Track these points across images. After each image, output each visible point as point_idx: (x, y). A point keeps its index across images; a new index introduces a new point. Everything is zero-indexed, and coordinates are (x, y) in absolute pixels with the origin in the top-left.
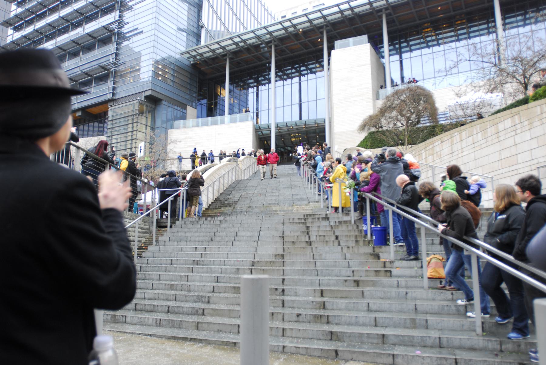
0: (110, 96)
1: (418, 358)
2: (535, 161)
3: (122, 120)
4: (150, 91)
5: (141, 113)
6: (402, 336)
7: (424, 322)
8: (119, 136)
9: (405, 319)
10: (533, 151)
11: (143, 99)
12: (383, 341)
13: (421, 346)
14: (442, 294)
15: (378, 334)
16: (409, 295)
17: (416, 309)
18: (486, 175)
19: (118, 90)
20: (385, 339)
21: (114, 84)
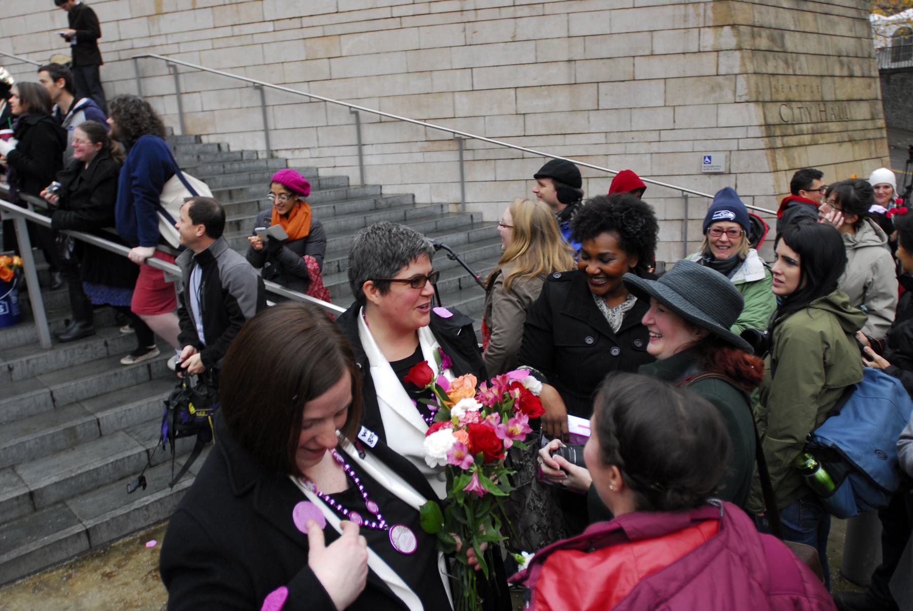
1: (137, 513)
2: (127, 45)
6: (72, 478)
7: (94, 426)
9: (53, 435)
10: (120, 23)
12: (34, 504)
13: (114, 481)
14: (89, 350)
15: (17, 498)
16: (17, 371)
17: (54, 400)
18: (24, 57)
20: (37, 500)
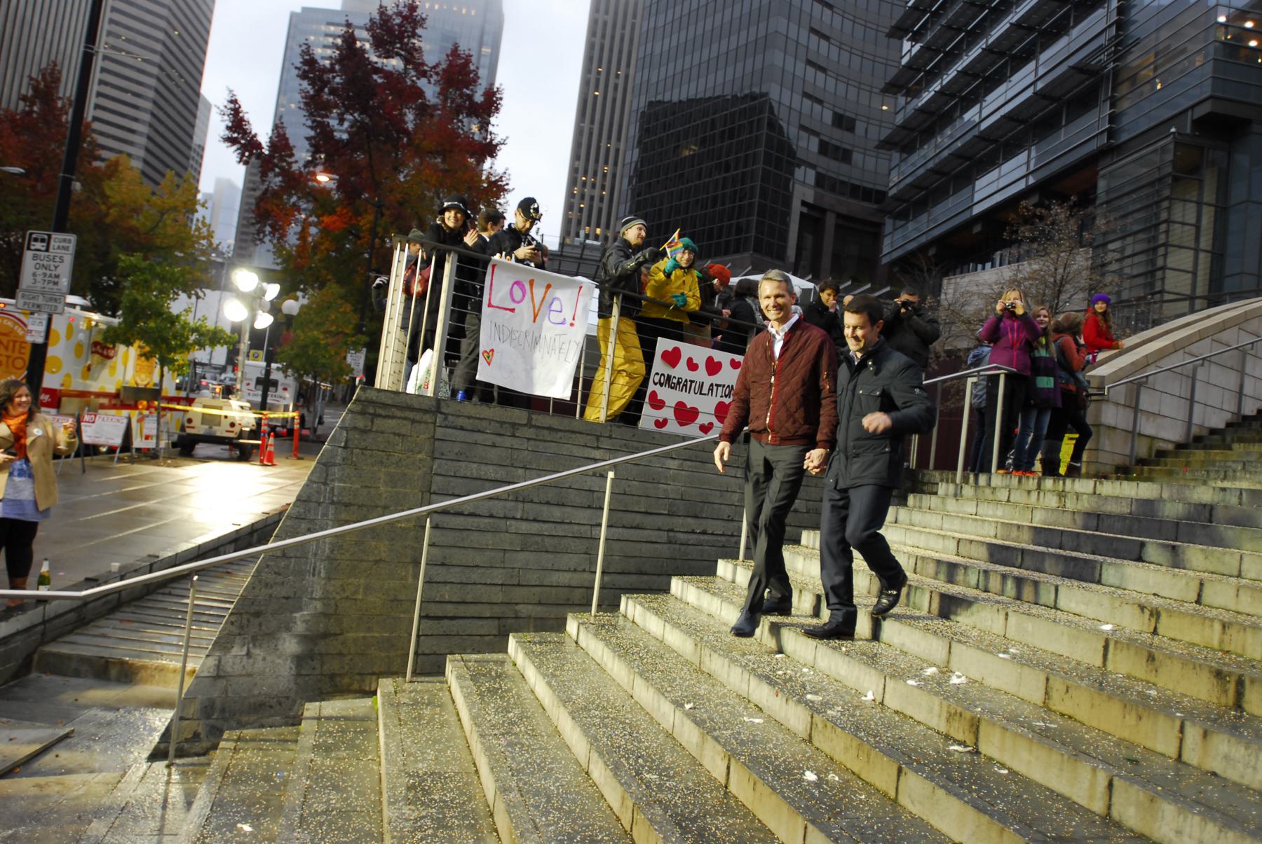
0: (1104, 139)
3: (1126, 200)
4: (1210, 102)
5: (1186, 172)
8: (1129, 240)
11: (1188, 131)
19: (1125, 121)
21: (1112, 106)
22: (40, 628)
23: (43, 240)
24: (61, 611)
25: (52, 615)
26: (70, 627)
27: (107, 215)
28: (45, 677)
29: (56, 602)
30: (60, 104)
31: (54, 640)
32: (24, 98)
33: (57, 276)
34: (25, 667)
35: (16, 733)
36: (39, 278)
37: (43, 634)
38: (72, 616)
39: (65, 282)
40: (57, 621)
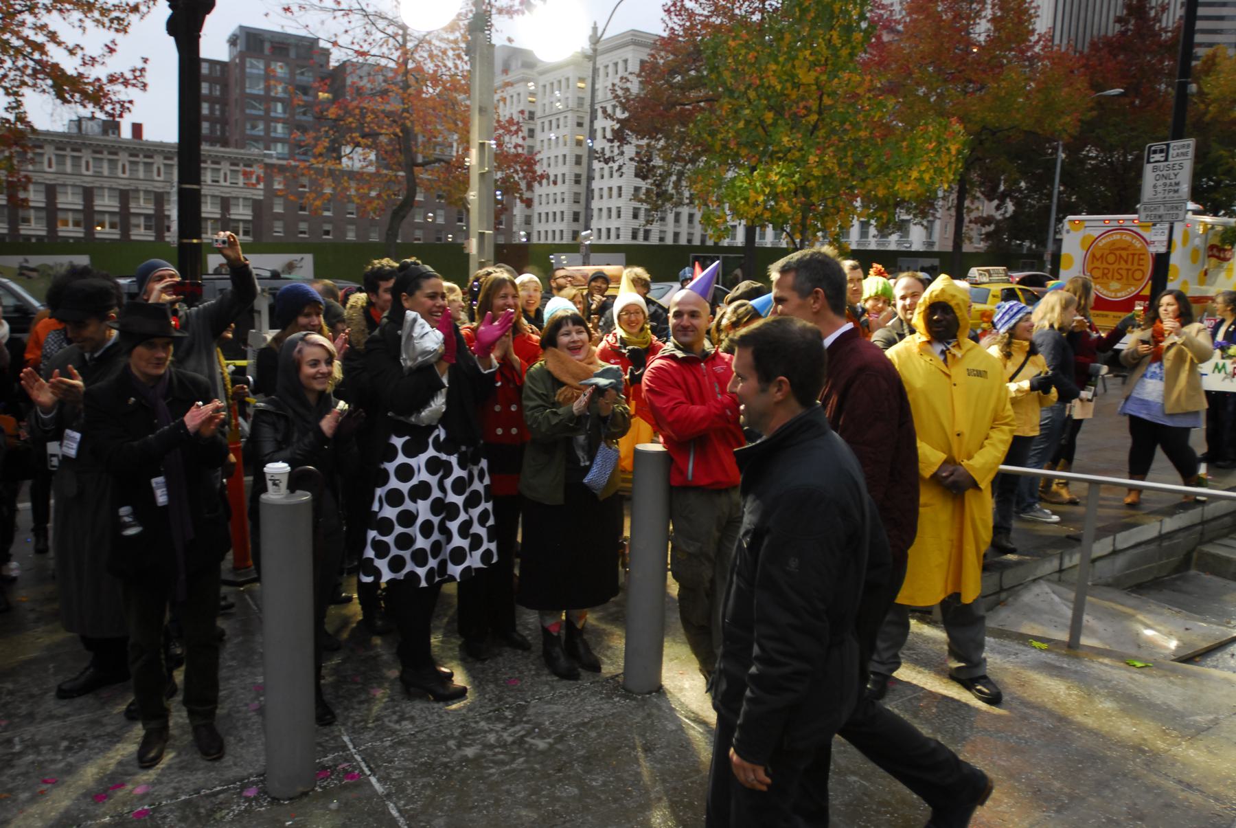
22: (1200, 527)
23: (1162, 151)
24: (1217, 514)
25: (1210, 517)
26: (1225, 531)
27: (1205, 114)
28: (1203, 575)
29: (1224, 503)
30: (1153, 13)
31: (1211, 541)
32: (1119, 20)
33: (1177, 184)
34: (1185, 564)
35: (1190, 624)
36: (1159, 189)
37: (1202, 534)
38: (1227, 520)
39: (1185, 188)
40: (1213, 524)
